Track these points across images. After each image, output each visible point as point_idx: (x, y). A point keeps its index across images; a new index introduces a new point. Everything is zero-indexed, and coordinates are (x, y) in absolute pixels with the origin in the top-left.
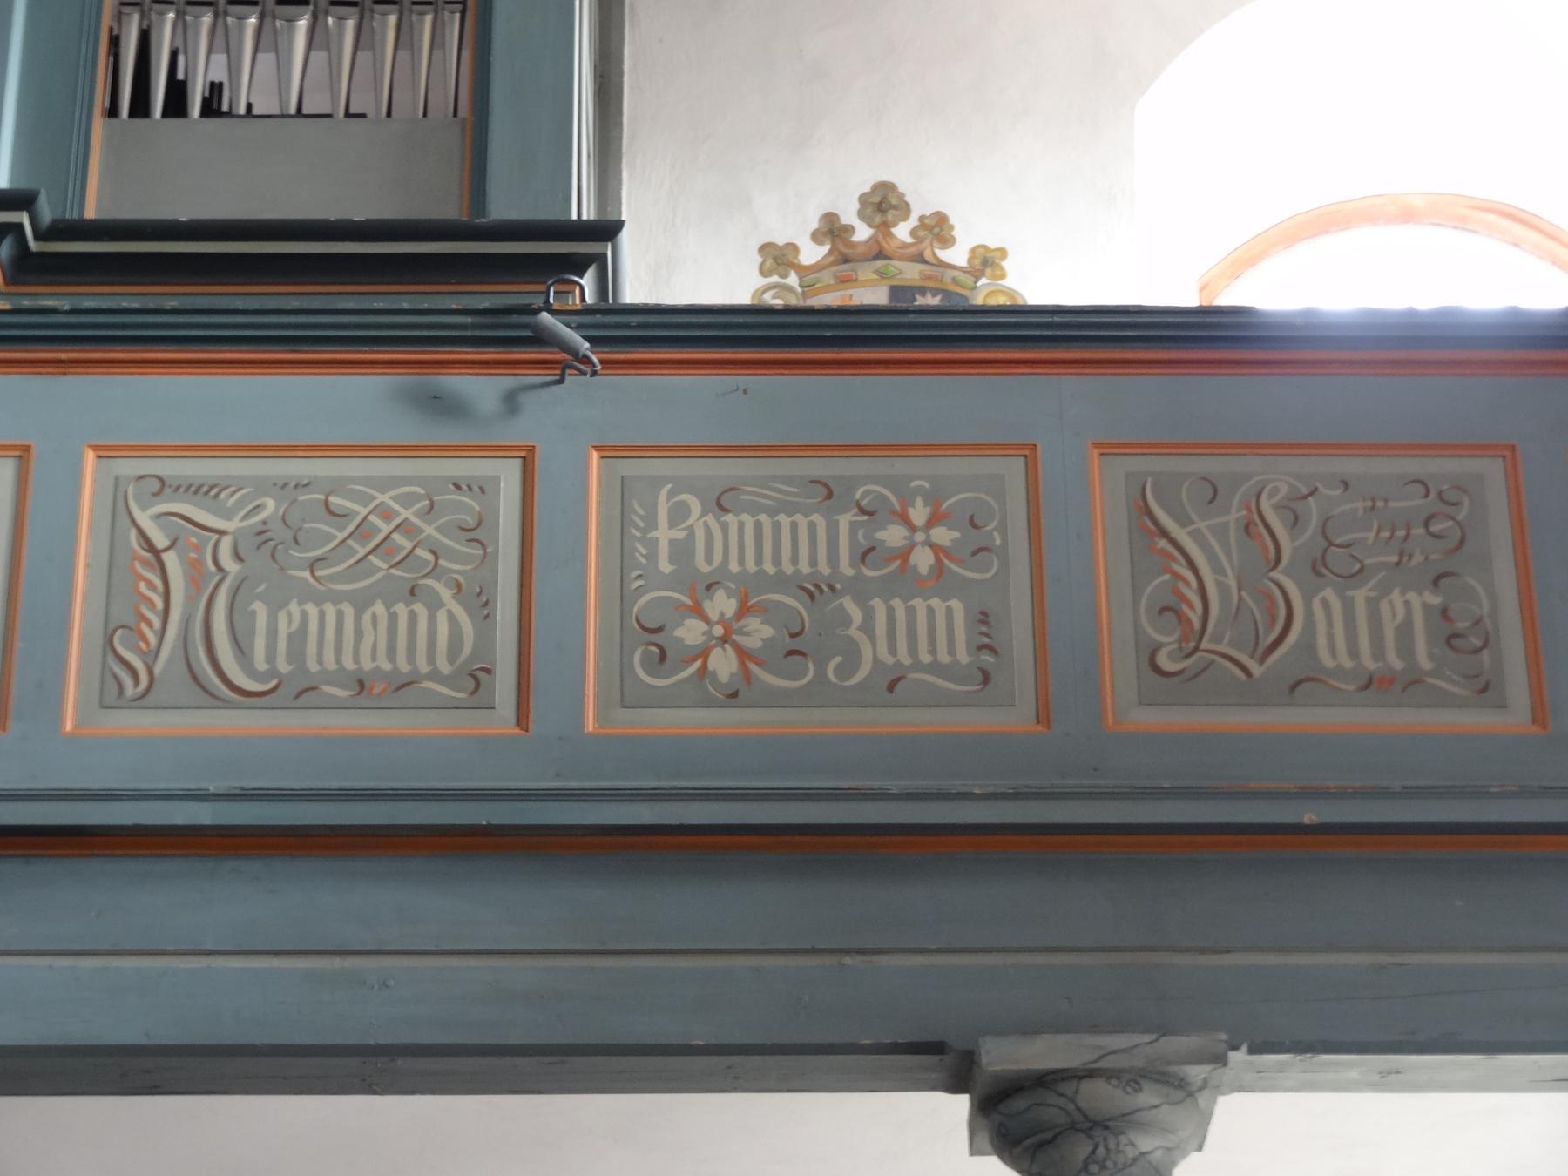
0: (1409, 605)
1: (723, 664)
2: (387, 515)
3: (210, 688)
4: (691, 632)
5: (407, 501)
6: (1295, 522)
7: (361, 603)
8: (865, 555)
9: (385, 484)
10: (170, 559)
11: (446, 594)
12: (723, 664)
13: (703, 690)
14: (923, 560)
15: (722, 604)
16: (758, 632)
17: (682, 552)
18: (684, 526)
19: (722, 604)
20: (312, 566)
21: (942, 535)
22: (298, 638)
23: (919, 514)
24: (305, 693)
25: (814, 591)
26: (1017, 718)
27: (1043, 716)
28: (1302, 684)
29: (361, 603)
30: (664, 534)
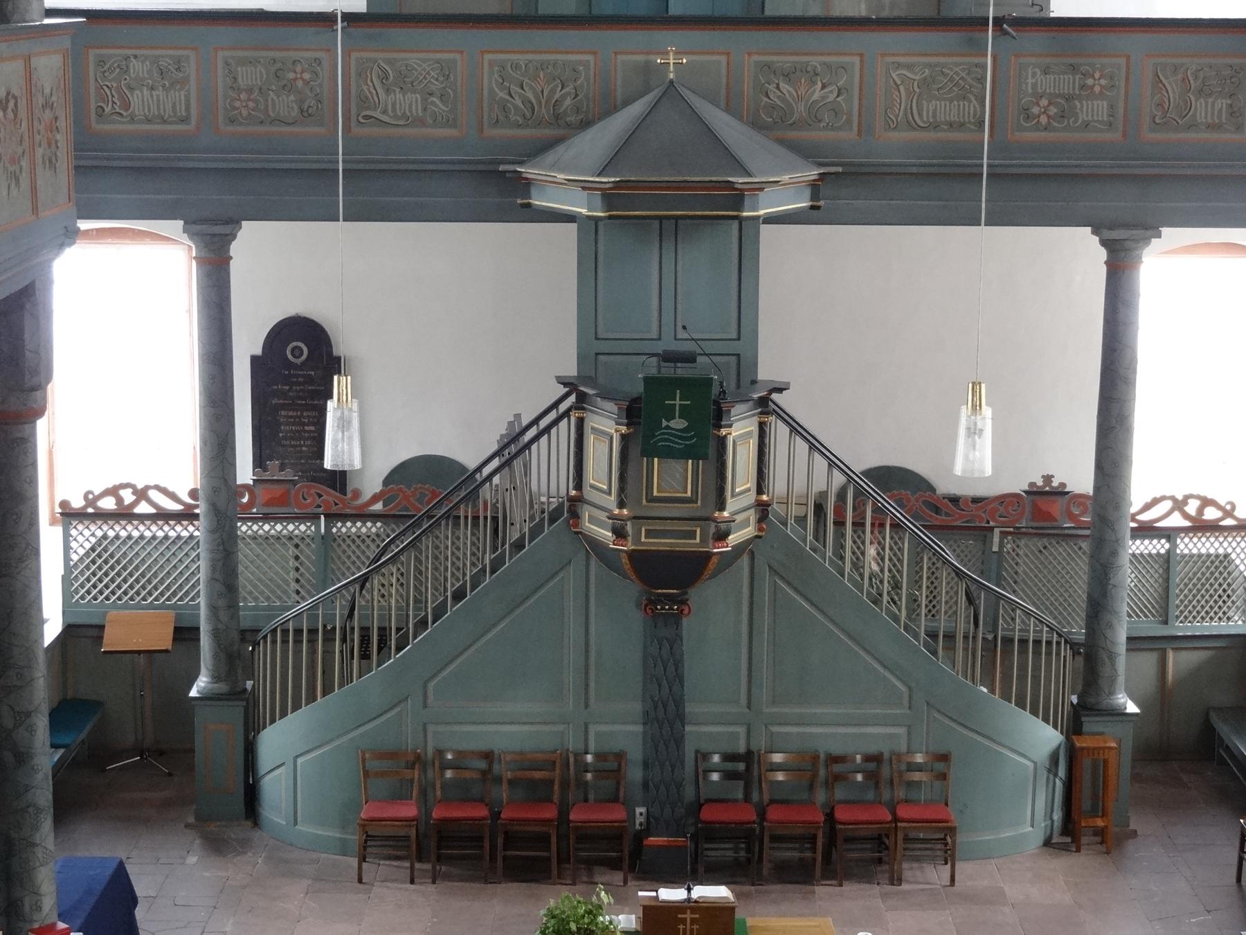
0: (1222, 103)
1: (1044, 119)
2: (956, 73)
3: (912, 126)
4: (1035, 110)
5: (963, 70)
6: (1196, 78)
7: (951, 101)
8: (1082, 87)
9: (957, 65)
10: (902, 88)
11: (973, 98)
12: (1044, 119)
13: (1038, 127)
14: (1097, 89)
15: (1044, 102)
16: (1053, 110)
17: (1034, 85)
18: (1034, 79)
19: (1044, 102)
20: (938, 90)
21: (1103, 82)
22: (935, 111)
23: (1097, 75)
24: (935, 126)
25: (1069, 98)
26: (1116, 136)
27: (1124, 135)
28: (1192, 126)
29: (951, 101)
30: (1030, 81)
